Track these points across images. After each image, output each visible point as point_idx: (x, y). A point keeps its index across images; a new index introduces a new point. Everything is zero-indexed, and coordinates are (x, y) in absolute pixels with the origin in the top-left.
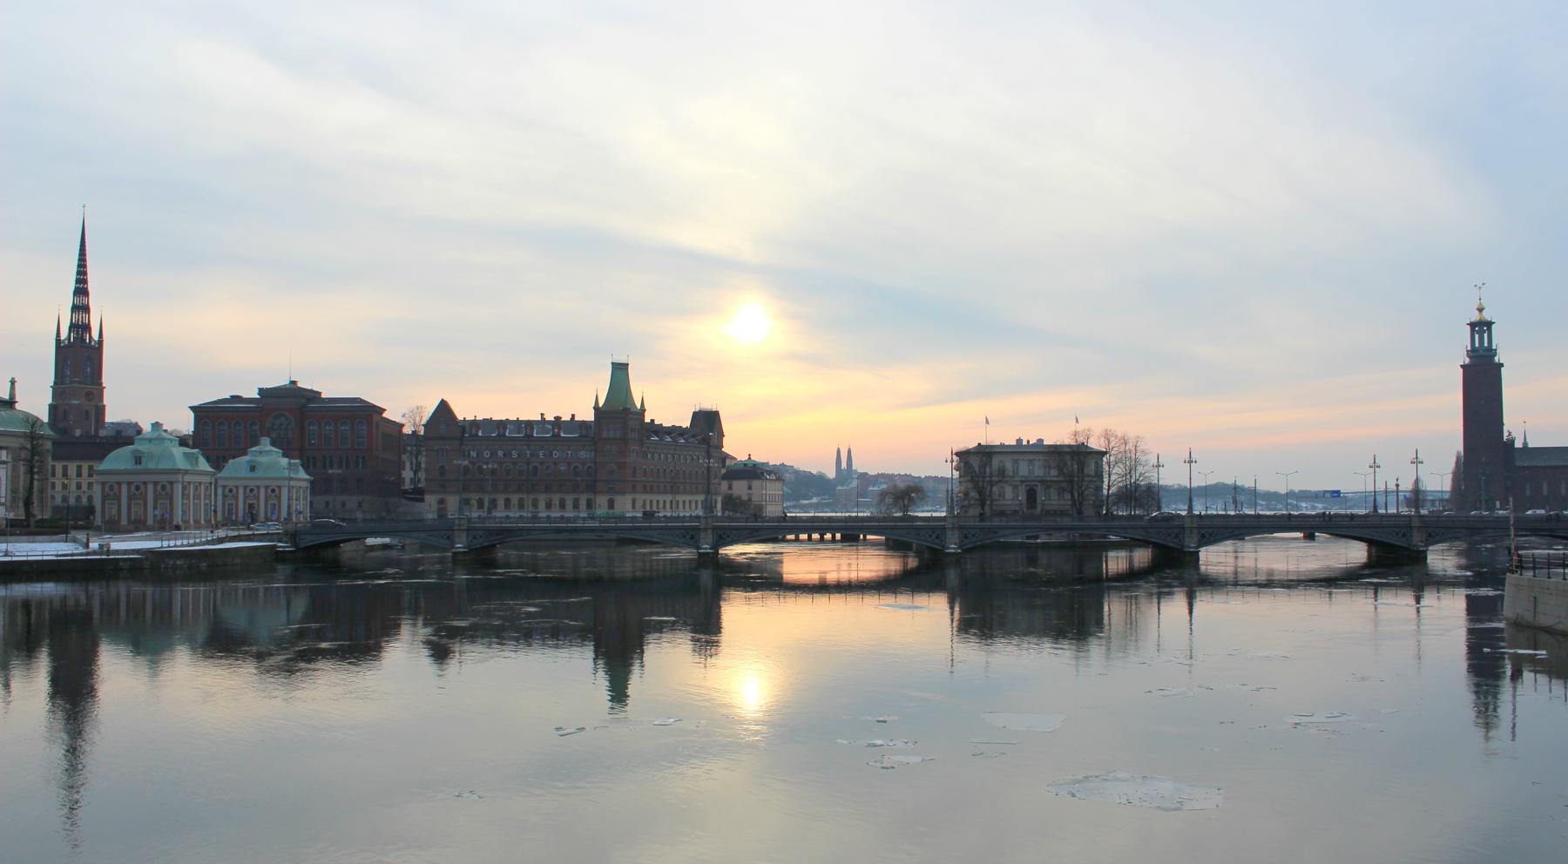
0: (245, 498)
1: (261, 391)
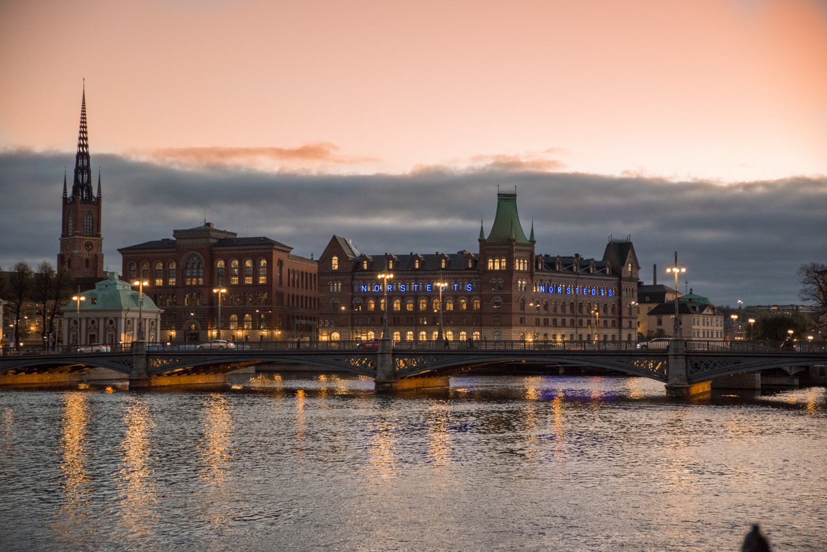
0: (87, 329)
1: (176, 233)
